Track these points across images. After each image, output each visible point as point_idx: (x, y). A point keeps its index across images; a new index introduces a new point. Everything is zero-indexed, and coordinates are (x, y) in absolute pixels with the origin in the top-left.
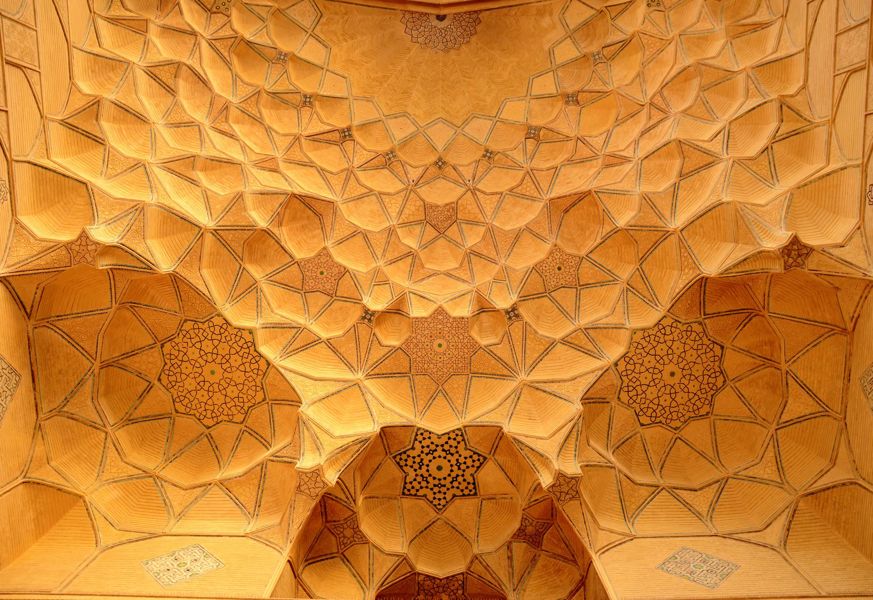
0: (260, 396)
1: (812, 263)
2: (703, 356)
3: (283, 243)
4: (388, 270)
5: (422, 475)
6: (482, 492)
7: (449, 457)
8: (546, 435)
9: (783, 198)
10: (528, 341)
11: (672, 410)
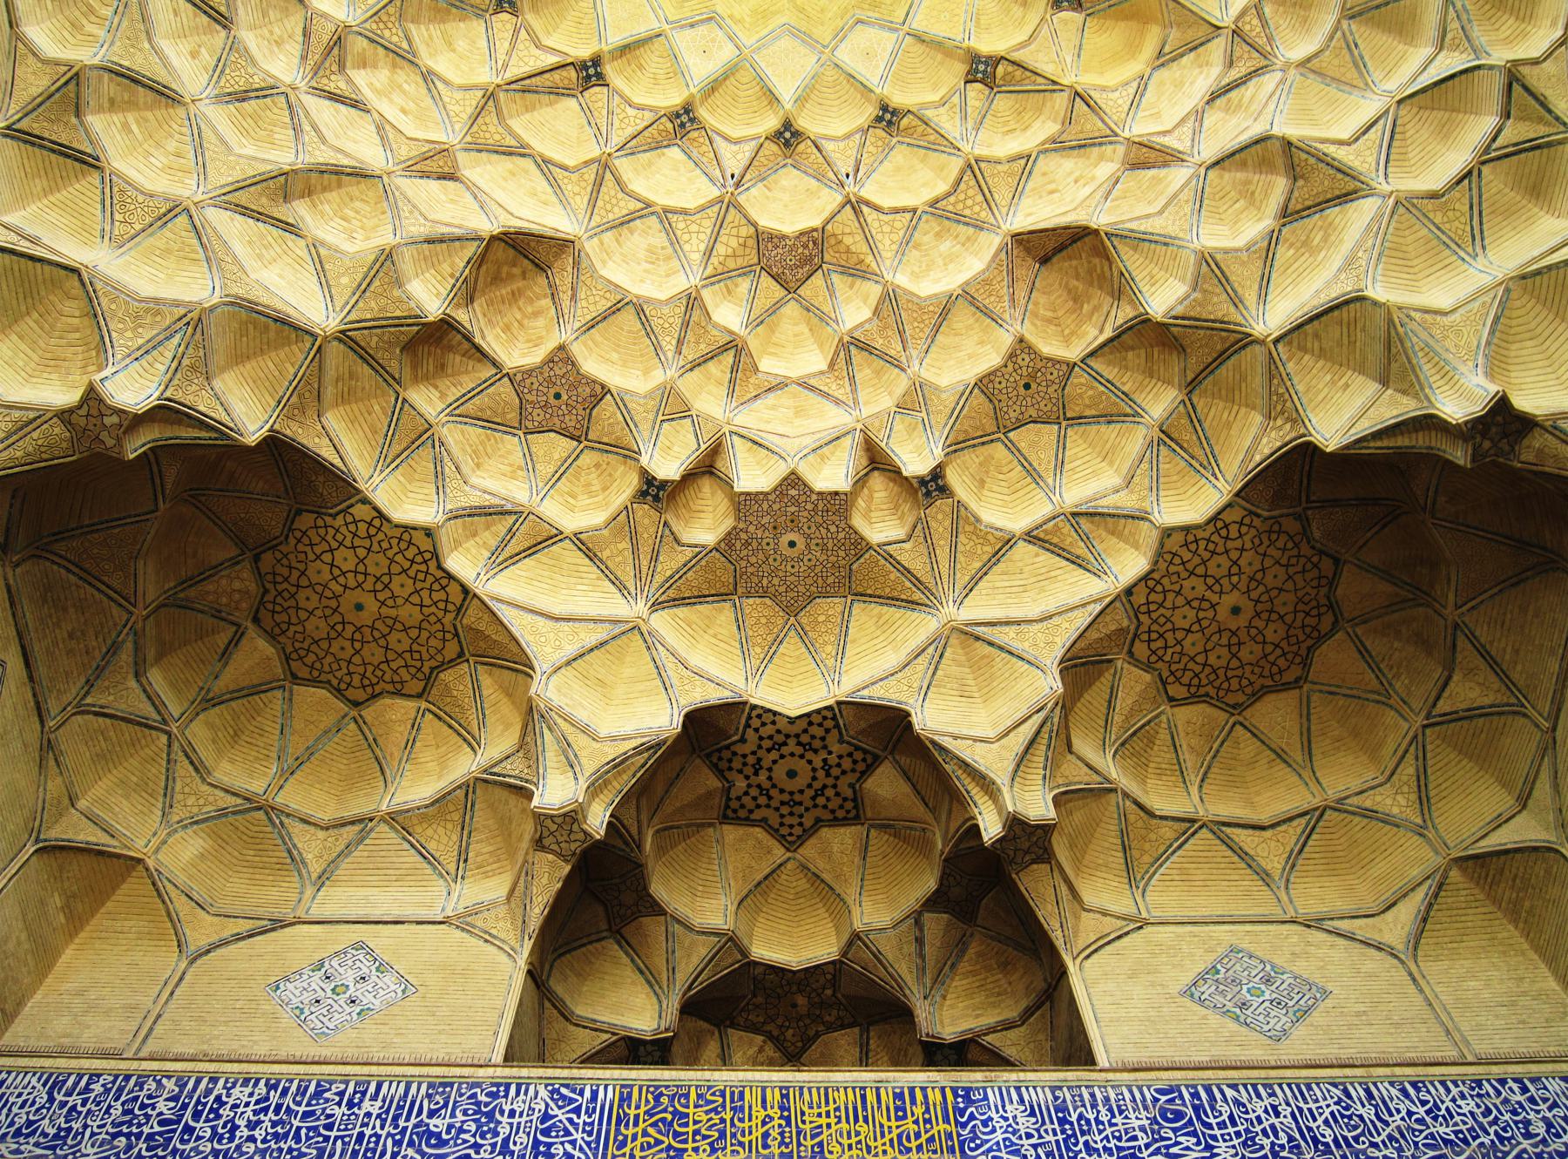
0: (452, 649)
2: (1298, 578)
3: (478, 340)
4: (689, 385)
5: (759, 786)
7: (810, 755)
8: (992, 734)
10: (962, 538)
11: (1230, 673)
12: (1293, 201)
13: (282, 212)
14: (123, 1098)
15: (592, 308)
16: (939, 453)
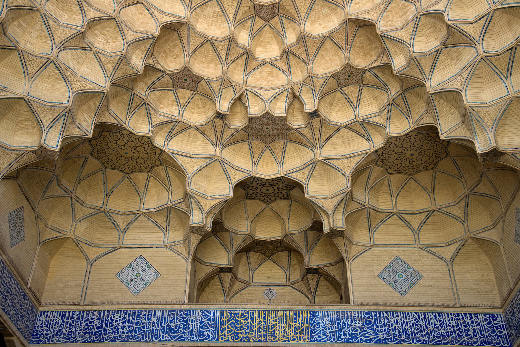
1: (502, 161)
2: (435, 147)
6: (292, 197)
9: (503, 103)
10: (323, 128)
12: (448, 41)
13: (83, 44)
14: (84, 320)
15: (195, 44)
16: (317, 101)
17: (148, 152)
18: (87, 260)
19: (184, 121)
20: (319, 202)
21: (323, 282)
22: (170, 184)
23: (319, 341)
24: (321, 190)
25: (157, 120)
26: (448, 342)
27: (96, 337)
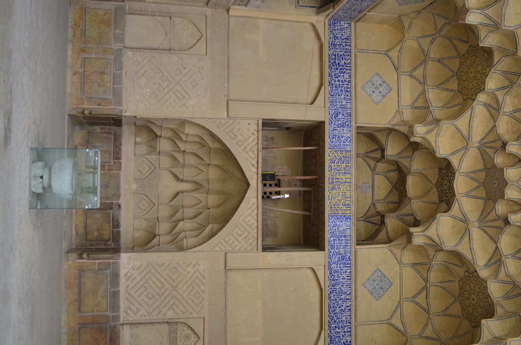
0: (465, 98)
10: (496, 229)
16: (518, 224)
17: (473, 90)
18: (388, 50)
19: (500, 117)
20: (434, 224)
21: (375, 228)
22: (448, 108)
23: (329, 222)
24: (443, 228)
25: (500, 95)
26: (330, 313)
27: (332, 63)
